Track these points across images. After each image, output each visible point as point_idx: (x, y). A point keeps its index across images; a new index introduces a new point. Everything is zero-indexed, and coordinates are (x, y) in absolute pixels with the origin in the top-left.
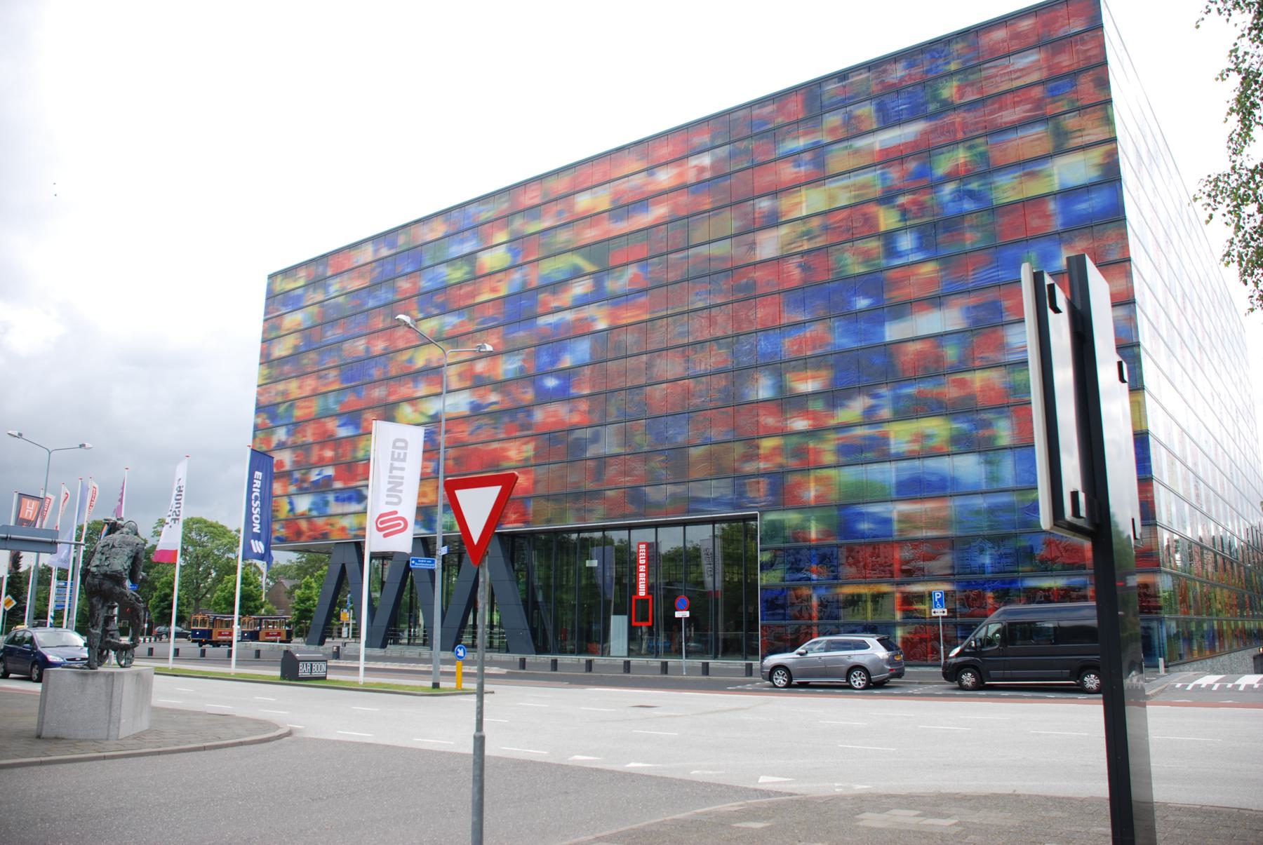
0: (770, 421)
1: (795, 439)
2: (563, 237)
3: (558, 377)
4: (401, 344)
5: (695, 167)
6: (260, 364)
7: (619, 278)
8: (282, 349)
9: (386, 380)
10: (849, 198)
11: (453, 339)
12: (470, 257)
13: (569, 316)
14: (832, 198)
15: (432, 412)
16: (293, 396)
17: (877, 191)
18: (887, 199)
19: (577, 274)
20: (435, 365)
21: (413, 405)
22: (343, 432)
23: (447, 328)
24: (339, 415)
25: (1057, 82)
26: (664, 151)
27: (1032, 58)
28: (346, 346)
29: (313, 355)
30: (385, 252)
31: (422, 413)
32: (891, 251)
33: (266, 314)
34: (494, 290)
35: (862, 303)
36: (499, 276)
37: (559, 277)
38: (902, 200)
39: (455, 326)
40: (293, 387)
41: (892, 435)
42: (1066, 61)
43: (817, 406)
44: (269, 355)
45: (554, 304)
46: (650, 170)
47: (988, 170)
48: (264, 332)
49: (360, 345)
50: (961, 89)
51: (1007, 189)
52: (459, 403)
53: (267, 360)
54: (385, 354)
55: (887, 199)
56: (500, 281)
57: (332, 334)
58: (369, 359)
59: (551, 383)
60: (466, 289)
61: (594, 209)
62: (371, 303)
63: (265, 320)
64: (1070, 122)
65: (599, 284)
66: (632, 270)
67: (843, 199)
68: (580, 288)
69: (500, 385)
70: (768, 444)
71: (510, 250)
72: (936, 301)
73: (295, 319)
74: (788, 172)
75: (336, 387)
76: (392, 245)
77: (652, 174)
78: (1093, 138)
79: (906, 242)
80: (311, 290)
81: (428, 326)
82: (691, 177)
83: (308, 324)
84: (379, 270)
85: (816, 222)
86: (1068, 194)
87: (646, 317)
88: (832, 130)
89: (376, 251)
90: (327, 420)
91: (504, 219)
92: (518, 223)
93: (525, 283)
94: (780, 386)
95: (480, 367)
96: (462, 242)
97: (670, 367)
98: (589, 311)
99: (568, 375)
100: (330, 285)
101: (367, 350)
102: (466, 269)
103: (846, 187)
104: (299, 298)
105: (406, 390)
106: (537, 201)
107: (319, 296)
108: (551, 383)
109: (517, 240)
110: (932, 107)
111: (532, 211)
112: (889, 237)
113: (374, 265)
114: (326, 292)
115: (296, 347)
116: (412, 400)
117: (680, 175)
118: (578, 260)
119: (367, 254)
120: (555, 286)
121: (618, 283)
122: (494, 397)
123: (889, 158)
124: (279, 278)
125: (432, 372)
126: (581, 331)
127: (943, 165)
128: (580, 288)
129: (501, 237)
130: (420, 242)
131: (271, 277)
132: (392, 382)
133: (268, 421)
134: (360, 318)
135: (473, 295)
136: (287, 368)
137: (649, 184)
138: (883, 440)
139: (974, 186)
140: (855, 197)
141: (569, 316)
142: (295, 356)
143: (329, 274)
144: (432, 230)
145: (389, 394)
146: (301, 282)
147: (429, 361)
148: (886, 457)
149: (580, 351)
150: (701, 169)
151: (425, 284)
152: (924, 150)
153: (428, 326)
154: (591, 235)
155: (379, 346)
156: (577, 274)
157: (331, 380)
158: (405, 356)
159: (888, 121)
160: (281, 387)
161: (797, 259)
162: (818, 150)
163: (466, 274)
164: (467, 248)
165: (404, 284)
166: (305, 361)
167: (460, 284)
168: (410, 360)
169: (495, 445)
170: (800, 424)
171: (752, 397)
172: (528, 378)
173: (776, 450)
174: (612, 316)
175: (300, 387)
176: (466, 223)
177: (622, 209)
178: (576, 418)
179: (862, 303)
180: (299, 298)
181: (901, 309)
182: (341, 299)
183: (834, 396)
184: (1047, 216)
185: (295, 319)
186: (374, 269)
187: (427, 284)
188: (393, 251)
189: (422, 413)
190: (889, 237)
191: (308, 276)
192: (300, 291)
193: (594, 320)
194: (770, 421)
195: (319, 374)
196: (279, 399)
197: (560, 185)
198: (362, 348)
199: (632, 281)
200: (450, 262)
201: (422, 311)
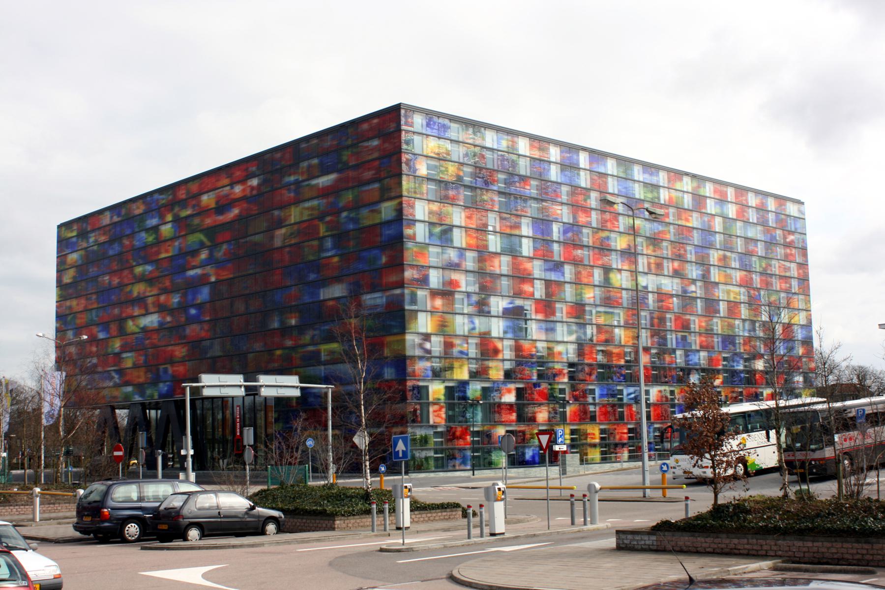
0: (276, 340)
1: (287, 351)
2: (196, 221)
3: (196, 309)
5: (250, 186)
7: (219, 251)
8: (67, 279)
10: (309, 215)
11: (149, 280)
12: (155, 229)
13: (198, 271)
15: (142, 326)
16: (74, 311)
18: (321, 218)
19: (202, 245)
22: (101, 336)
23: (147, 273)
24: (98, 325)
27: (375, 143)
29: (83, 284)
30: (116, 219)
31: (137, 326)
33: (58, 253)
34: (167, 251)
35: (312, 277)
36: (169, 243)
37: (196, 247)
38: (328, 219)
39: (151, 272)
40: (74, 303)
41: (323, 351)
45: (194, 264)
46: (232, 185)
47: (356, 206)
48: (57, 265)
51: (367, 218)
52: (151, 320)
53: (60, 284)
54: (121, 286)
56: (169, 246)
57: (93, 271)
58: (110, 289)
59: (193, 311)
60: (154, 249)
61: (208, 206)
62: (111, 253)
63: (58, 257)
65: (211, 255)
66: (225, 247)
68: (204, 255)
69: (171, 311)
70: (278, 352)
71: (173, 227)
73: (73, 257)
75: (95, 306)
76: (119, 215)
77: (232, 188)
79: (329, 243)
80: (80, 240)
81: (139, 270)
83: (80, 262)
84: (113, 230)
87: (231, 276)
89: (112, 217)
90: (93, 327)
91: (170, 206)
92: (176, 209)
93: (180, 249)
94: (282, 322)
95: (162, 298)
96: (152, 217)
97: (240, 307)
98: (209, 269)
99: (199, 307)
100: (90, 237)
101: (110, 283)
102: (154, 236)
103: (308, 209)
104: (75, 243)
105: (129, 311)
106: (184, 197)
107: (85, 245)
108: (193, 311)
109: (177, 220)
111: (183, 204)
113: (111, 227)
114: (88, 242)
115: (74, 277)
116: (133, 318)
117: (244, 190)
118: (201, 237)
119: (106, 220)
120: (195, 253)
121: (220, 254)
122: (169, 319)
123: (325, 192)
124: (63, 229)
125: (140, 301)
126: (203, 280)
128: (204, 255)
129: (169, 218)
130: (132, 215)
131: (59, 227)
133: (63, 326)
134: (106, 261)
135: (159, 253)
136: (71, 291)
138: (318, 352)
140: (311, 215)
141: (198, 271)
142: (74, 283)
143: (89, 229)
144: (138, 208)
146: (74, 234)
147: (139, 293)
148: (320, 363)
149: (204, 294)
151: (137, 243)
153: (139, 270)
154: (208, 221)
155: (116, 281)
156: (202, 245)
158: (128, 289)
160: (68, 303)
161: (287, 249)
163: (154, 239)
164: (154, 222)
165: (126, 242)
167: (152, 245)
168: (131, 292)
169: (170, 348)
170: (289, 343)
171: (272, 327)
172: (183, 307)
174: (217, 274)
175: (78, 305)
176: (154, 206)
177: (222, 207)
178: (203, 334)
179: (312, 277)
180: (75, 243)
182: (95, 248)
183: (301, 329)
185: (73, 257)
186: (110, 230)
187: (138, 243)
188: (119, 219)
189: (137, 326)
191: (78, 229)
192: (74, 240)
193: (210, 275)
194: (276, 340)
195: (87, 296)
196: (67, 312)
197: (194, 187)
198: (107, 281)
199: (225, 254)
200: (147, 230)
201: (135, 261)
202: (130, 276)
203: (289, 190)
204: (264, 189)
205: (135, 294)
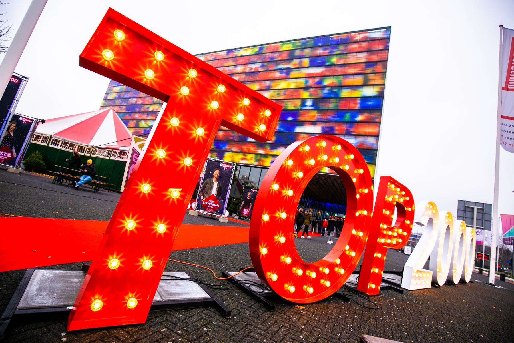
0: (252, 149)
4: (147, 103)
6: (103, 100)
8: (110, 97)
9: (139, 112)
14: (289, 85)
17: (303, 86)
20: (155, 111)
21: (145, 122)
25: (369, 64)
26: (241, 61)
28: (130, 100)
32: (303, 105)
38: (311, 90)
42: (374, 58)
43: (268, 148)
44: (106, 98)
46: (236, 66)
47: (341, 87)
49: (134, 101)
50: (338, 60)
53: (105, 99)
54: (142, 104)
55: (306, 88)
58: (136, 105)
64: (371, 76)
67: (293, 86)
72: (314, 123)
74: (277, 75)
75: (124, 111)
77: (236, 67)
78: (376, 83)
79: (309, 103)
82: (247, 70)
85: (282, 92)
86: (364, 99)
88: (295, 65)
101: (136, 102)
103: (295, 83)
105: (145, 117)
110: (328, 64)
112: (304, 101)
116: (145, 120)
117: (245, 69)
123: (309, 77)
127: (327, 82)
132: (140, 114)
137: (235, 70)
139: (335, 90)
140: (296, 86)
145: (139, 117)
147: (154, 109)
150: (251, 69)
152: (322, 76)
155: (140, 102)
157: (123, 109)
159: (313, 64)
162: (289, 70)
166: (117, 102)
168: (148, 108)
170: (261, 152)
173: (251, 159)
181: (302, 123)
184: (356, 104)
189: (147, 125)
190: (304, 101)
194: (252, 149)
202: (150, 101)
203: (281, 73)
204: (260, 70)
205: (151, 109)
